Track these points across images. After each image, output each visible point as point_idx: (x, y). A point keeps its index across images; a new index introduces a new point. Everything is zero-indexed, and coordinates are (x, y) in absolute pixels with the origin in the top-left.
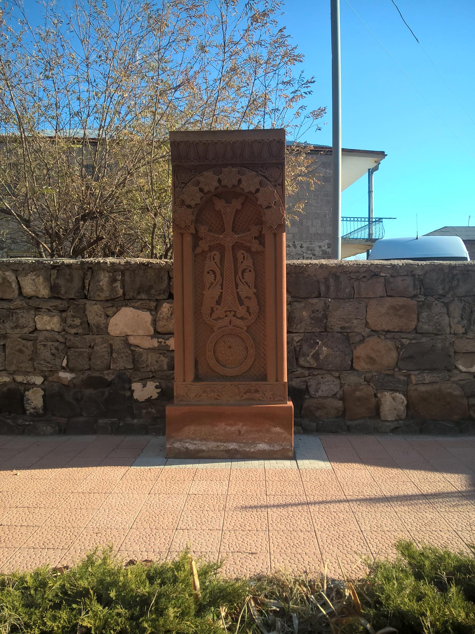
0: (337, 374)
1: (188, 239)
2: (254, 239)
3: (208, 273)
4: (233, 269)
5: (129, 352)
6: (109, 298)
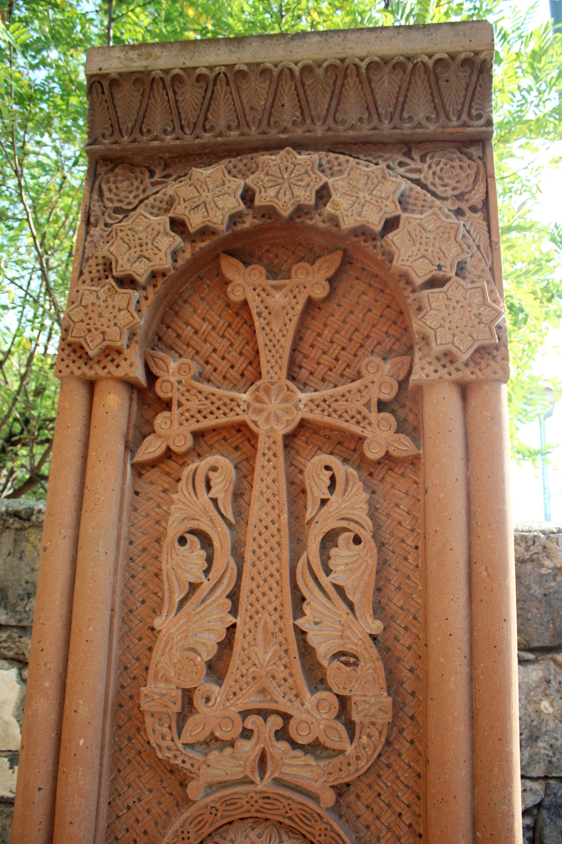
1: (114, 404)
2: (374, 408)
3: (182, 541)
4: (285, 531)
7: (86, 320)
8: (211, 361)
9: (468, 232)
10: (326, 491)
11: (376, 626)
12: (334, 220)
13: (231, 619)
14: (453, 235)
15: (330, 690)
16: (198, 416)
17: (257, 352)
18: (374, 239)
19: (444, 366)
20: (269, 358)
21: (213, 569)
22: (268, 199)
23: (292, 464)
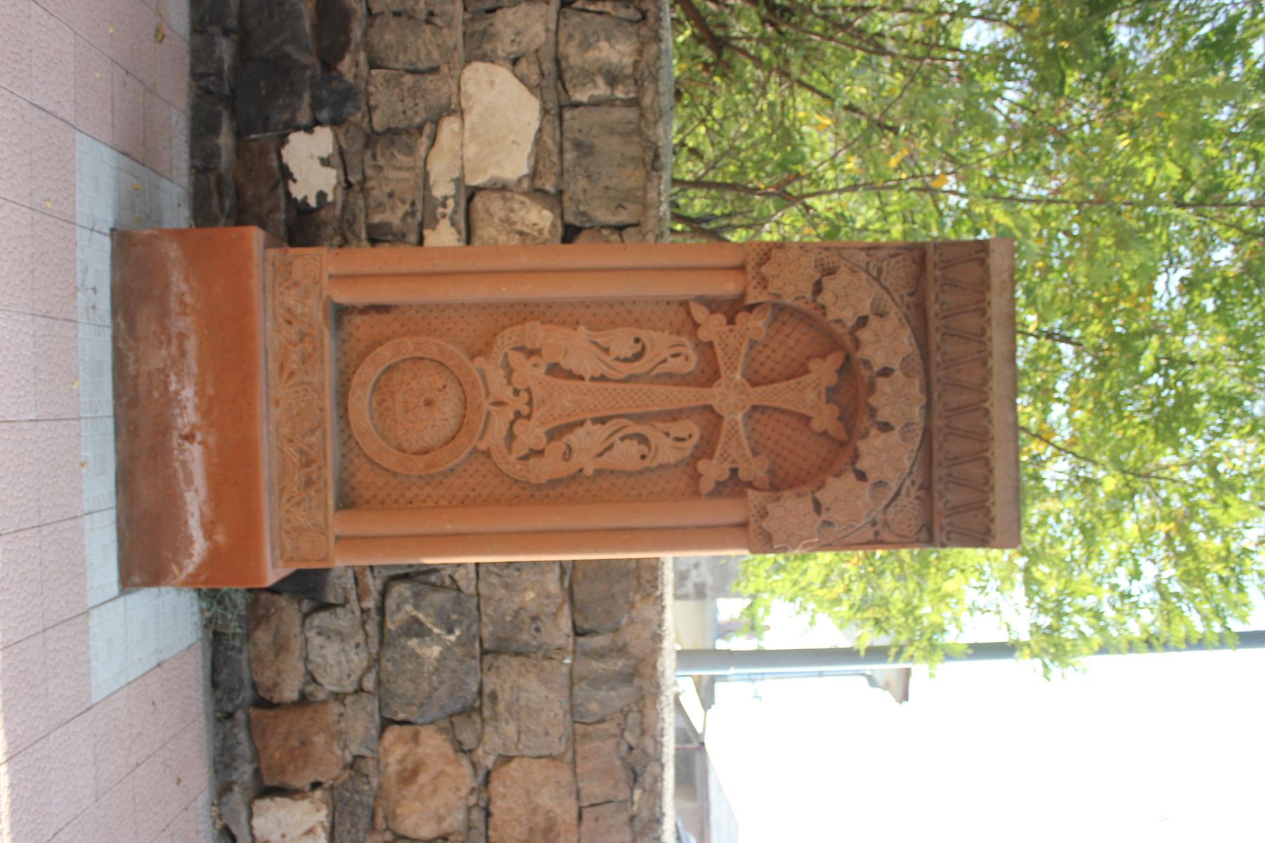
0: (369, 684)
1: (728, 287)
3: (637, 340)
5: (418, 120)
6: (564, 64)
11: (589, 471)
12: (865, 435)
13: (587, 377)
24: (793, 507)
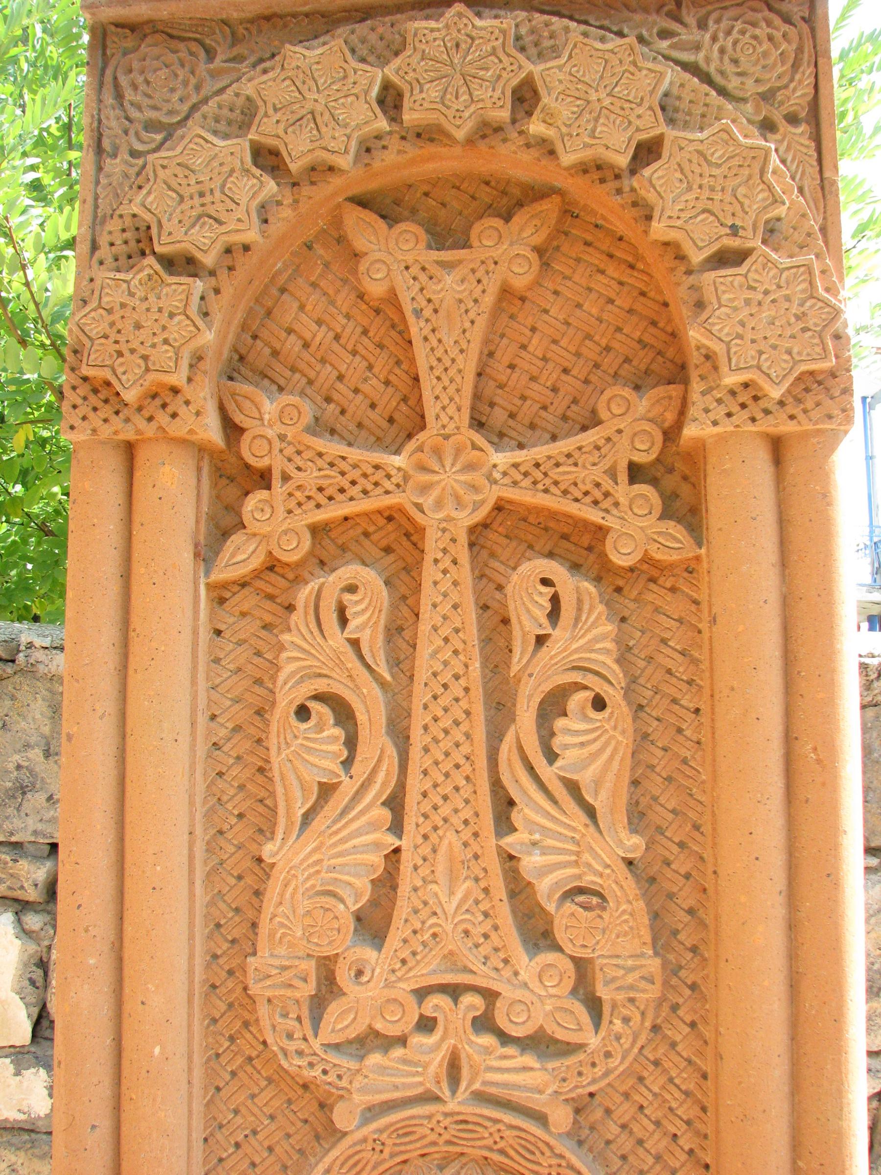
2: (623, 476)
3: (303, 712)
4: (477, 692)
7: (113, 336)
8: (335, 396)
9: (783, 162)
10: (545, 621)
13: (392, 841)
14: (757, 171)
15: (560, 949)
16: (321, 498)
17: (416, 379)
18: (617, 177)
19: (743, 406)
20: (438, 390)
21: (358, 758)
22: (426, 105)
23: (482, 576)
24: (729, 324)
